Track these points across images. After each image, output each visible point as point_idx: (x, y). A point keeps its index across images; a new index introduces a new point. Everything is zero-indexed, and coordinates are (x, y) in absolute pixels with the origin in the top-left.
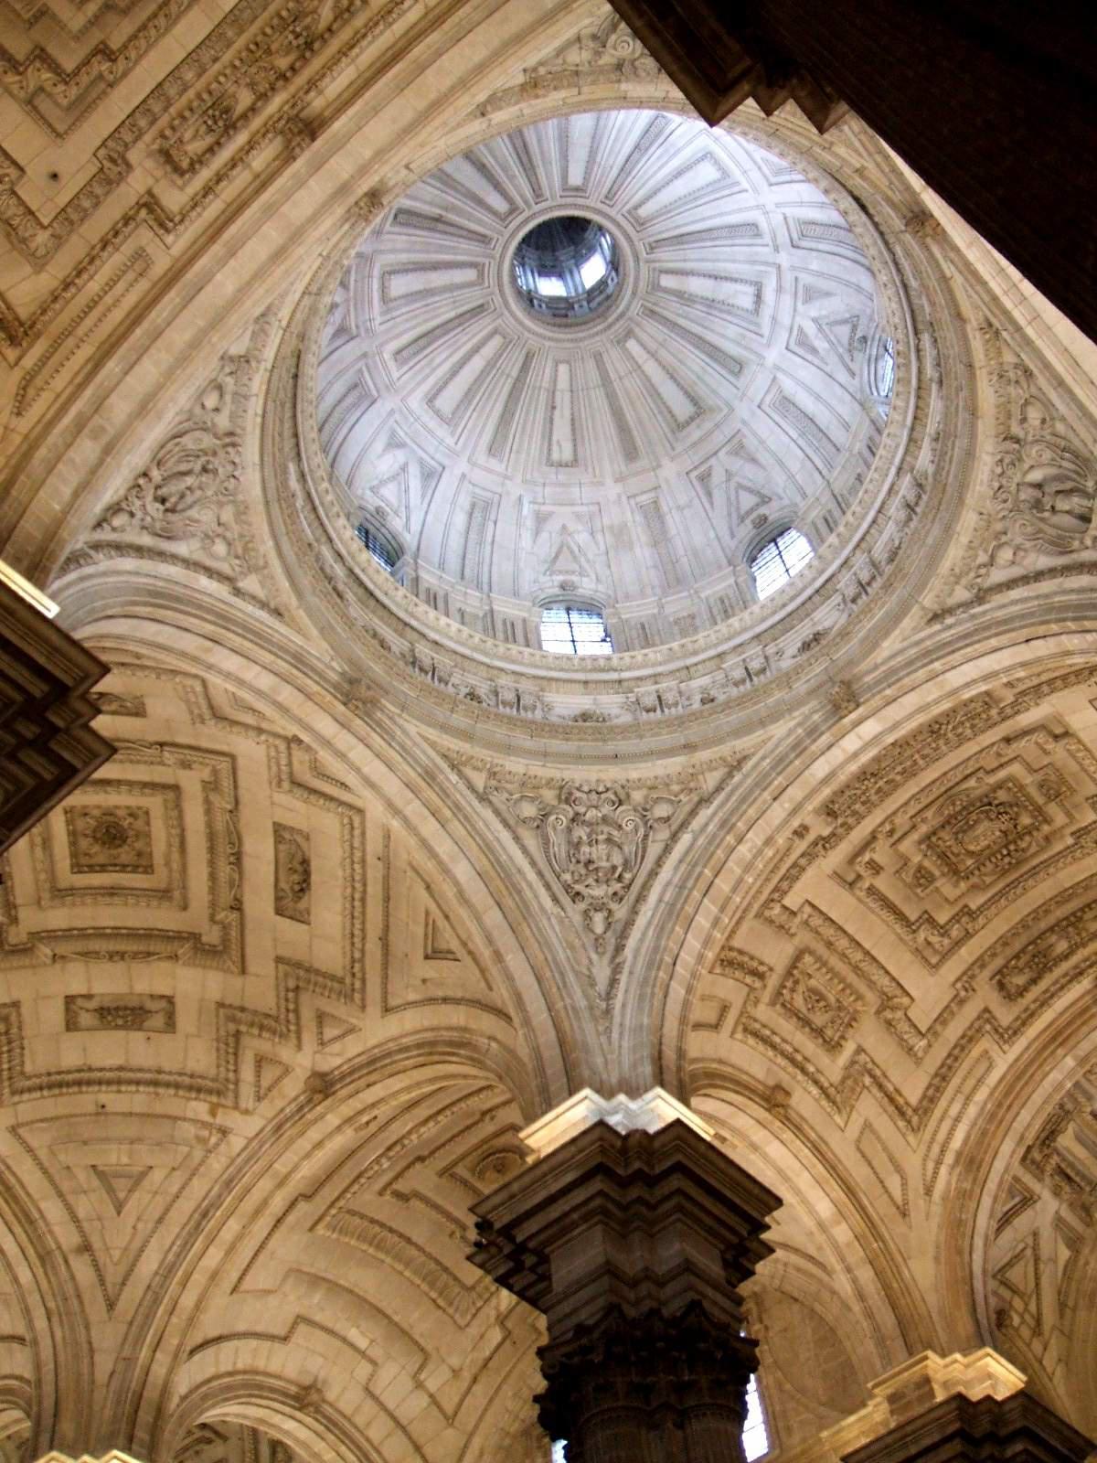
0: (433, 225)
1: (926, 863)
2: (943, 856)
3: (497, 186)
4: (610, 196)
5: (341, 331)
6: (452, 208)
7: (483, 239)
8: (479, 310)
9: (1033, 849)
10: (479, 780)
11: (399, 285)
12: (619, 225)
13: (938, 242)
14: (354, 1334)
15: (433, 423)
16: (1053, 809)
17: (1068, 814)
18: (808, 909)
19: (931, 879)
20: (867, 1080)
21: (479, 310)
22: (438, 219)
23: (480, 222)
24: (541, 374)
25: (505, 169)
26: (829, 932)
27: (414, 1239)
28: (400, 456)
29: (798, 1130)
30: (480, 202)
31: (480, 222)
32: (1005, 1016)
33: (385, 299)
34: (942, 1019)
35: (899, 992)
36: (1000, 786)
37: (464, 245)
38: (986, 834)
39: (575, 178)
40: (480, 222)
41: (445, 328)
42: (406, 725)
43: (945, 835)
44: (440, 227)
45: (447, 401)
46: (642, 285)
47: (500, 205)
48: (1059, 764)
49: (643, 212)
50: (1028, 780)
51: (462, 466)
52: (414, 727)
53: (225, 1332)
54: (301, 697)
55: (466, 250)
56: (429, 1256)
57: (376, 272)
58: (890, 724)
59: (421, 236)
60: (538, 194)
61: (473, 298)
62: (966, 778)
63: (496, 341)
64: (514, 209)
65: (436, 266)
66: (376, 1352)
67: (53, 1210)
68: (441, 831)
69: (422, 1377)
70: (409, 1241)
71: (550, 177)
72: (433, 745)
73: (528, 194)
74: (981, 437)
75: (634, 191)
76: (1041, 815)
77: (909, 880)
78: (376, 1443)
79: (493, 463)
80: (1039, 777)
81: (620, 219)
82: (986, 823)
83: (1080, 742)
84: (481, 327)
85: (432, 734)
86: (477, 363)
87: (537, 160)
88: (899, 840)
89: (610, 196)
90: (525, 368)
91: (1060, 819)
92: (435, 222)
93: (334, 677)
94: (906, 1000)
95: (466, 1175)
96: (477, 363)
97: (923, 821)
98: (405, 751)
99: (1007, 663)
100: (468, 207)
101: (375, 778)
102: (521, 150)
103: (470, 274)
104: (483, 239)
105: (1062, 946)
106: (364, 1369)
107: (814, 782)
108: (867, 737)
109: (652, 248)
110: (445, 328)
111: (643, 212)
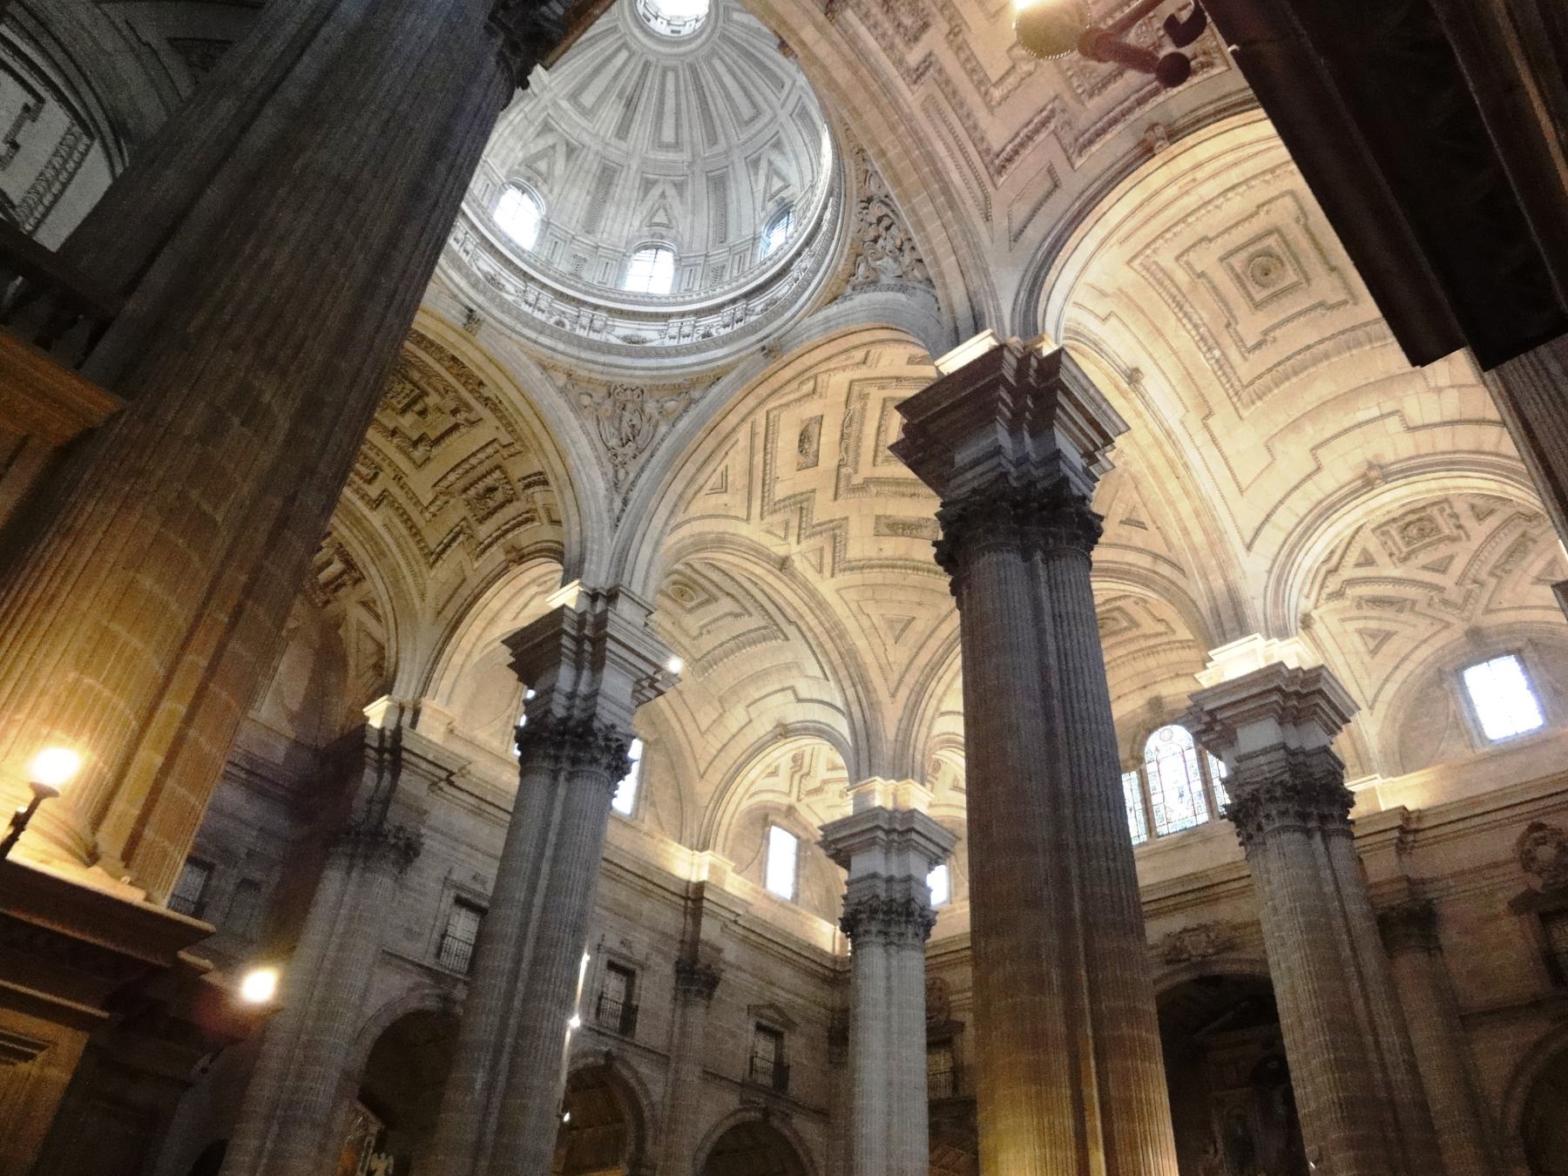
0: (632, 107)
3: (609, 60)
11: (668, 135)
14: (1362, 416)
15: (758, 125)
22: (628, 105)
27: (1311, 342)
28: (763, 164)
30: (620, 71)
31: (633, 71)
33: (677, 145)
37: (648, 84)
44: (635, 100)
47: (624, 55)
51: (783, 116)
53: (1268, 511)
55: (653, 79)
56: (1333, 336)
59: (638, 117)
63: (717, 63)
64: (625, 45)
65: (661, 102)
66: (1389, 406)
67: (1131, 557)
69: (1433, 385)
70: (1309, 347)
73: (611, 39)
78: (1450, 448)
79: (787, 88)
90: (734, 44)
92: (630, 104)
95: (1265, 293)
96: (728, 80)
100: (622, 80)
103: (670, 76)
104: (647, 65)
106: (1393, 424)
108: (818, 35)
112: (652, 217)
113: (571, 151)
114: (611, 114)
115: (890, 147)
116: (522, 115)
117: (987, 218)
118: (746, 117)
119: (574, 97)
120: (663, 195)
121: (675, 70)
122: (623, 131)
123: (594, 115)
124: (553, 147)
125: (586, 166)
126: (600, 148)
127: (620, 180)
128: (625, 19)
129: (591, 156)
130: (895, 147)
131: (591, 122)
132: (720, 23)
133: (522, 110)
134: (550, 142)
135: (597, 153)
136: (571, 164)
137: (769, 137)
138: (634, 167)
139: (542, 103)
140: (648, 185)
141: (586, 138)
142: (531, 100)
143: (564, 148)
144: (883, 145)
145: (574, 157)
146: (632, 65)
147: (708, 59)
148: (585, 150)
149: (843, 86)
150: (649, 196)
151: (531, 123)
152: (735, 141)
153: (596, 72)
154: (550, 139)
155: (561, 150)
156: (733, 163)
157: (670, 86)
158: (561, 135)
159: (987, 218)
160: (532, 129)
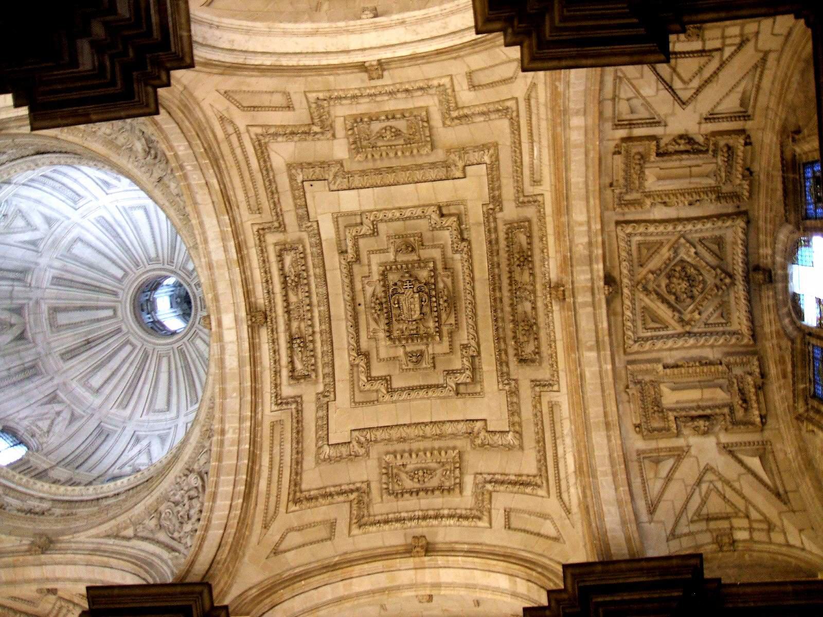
0: (88, 346)
1: (408, 349)
2: (411, 338)
3: (98, 308)
4: (137, 265)
5: (73, 418)
6: (90, 332)
7: (119, 330)
8: (146, 356)
9: (449, 281)
10: (130, 532)
11: (96, 381)
12: (154, 270)
13: (7, 128)
15: (161, 416)
16: (425, 253)
17: (434, 246)
18: (356, 434)
19: (421, 354)
20: (489, 487)
21: (146, 356)
23: (107, 326)
24: (192, 355)
25: (90, 299)
26: (395, 434)
29: (451, 551)
30: (99, 320)
31: (107, 326)
32: (543, 374)
34: (514, 411)
35: (470, 424)
36: (384, 275)
37: (110, 341)
38: (410, 303)
39: (119, 273)
40: (107, 327)
41: (137, 377)
42: (79, 539)
43: (396, 326)
44: (93, 344)
45: (161, 402)
46: (187, 279)
47: (109, 313)
48: (391, 232)
49: (153, 255)
50: (391, 256)
52: (82, 537)
54: (11, 570)
55: (114, 342)
57: (74, 384)
58: (232, 308)
60: (115, 294)
61: (137, 356)
62: (363, 290)
63: (165, 362)
68: (113, 571)
71: (110, 284)
72: (97, 536)
73: (112, 298)
74: (119, 163)
75: (139, 253)
76: (422, 263)
77: (411, 366)
80: (392, 250)
81: (149, 267)
82: (402, 298)
83: (371, 211)
84: (152, 364)
85: (93, 532)
86: (164, 377)
87: (98, 284)
88: (378, 355)
89: (137, 265)
90: (185, 359)
91: (436, 254)
92: (88, 344)
93: (26, 548)
94: (479, 425)
96: (164, 377)
97: (375, 331)
98: (76, 551)
99: (215, 222)
101: (75, 576)
102: (85, 286)
103: (128, 348)
104: (119, 330)
105: (528, 306)
107: (237, 371)
108: (233, 325)
109: (171, 262)
110: (137, 377)
111: (153, 255)
112: (39, 420)
113: (21, 337)
114: (69, 339)
115: (231, 431)
116: (10, 288)
117: (266, 526)
118: (157, 407)
119: (55, 310)
120: (58, 414)
121: (134, 347)
122: (70, 354)
123: (58, 331)
124: (12, 325)
125: (23, 354)
126: (43, 353)
127: (37, 381)
128: (127, 293)
129: (34, 350)
130: (234, 433)
131: (52, 332)
132: (185, 339)
133: (12, 286)
134: (13, 321)
135: (39, 353)
136: (13, 344)
137: (161, 428)
138: (55, 382)
139: (31, 295)
140: (53, 399)
141: (39, 338)
142: (25, 286)
143: (19, 332)
144: (227, 427)
145: (20, 342)
146: (108, 322)
147: (160, 358)
148: (31, 345)
149: (227, 370)
150: (49, 406)
151: (11, 298)
152: (137, 416)
153: (82, 308)
154: (14, 319)
155: (16, 331)
156: (124, 428)
157: (123, 354)
158: (25, 324)
159: (266, 526)
160: (9, 302)
